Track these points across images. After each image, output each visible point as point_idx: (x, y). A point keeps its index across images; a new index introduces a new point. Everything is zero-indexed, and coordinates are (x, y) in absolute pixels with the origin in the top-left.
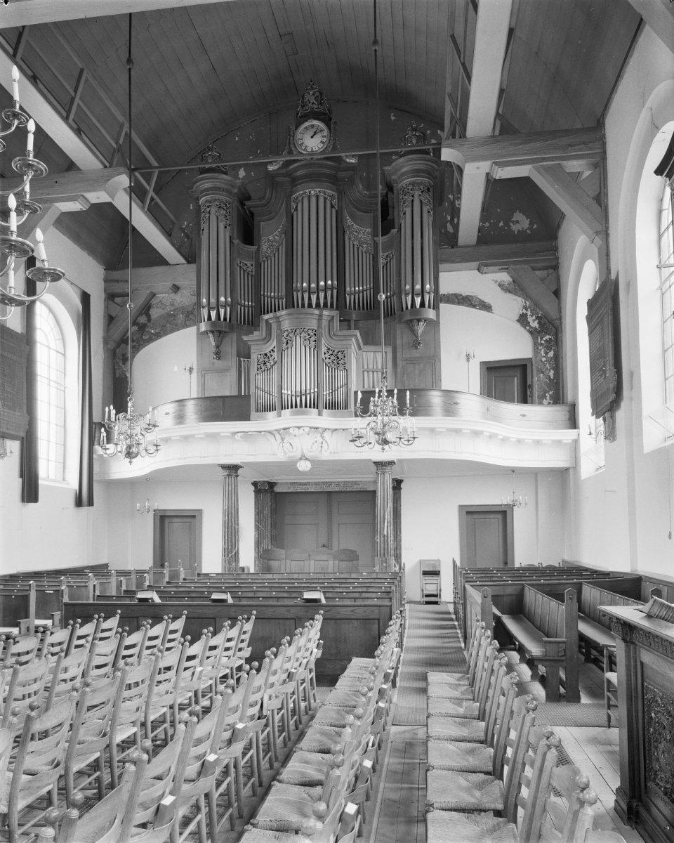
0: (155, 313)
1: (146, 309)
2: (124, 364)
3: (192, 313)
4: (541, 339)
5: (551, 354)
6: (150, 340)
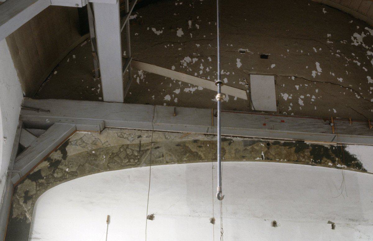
0: (71, 150)
1: (63, 147)
2: (25, 202)
6: (64, 178)
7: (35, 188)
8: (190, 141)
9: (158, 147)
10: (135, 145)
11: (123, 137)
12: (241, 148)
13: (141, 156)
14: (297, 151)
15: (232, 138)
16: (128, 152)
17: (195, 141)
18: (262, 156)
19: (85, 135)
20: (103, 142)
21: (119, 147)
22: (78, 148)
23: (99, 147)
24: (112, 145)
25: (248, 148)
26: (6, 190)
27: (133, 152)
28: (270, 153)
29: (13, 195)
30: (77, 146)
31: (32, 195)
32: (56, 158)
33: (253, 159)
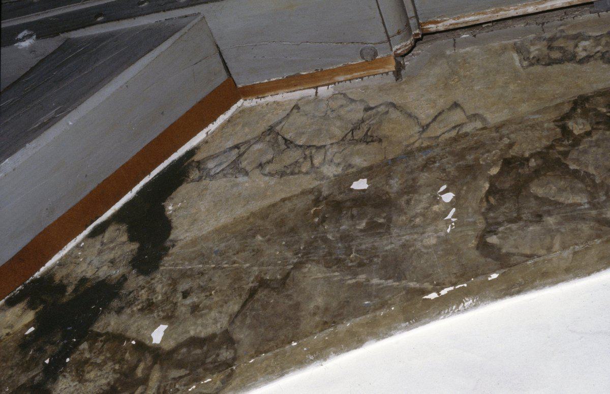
19: (297, 107)
20: (425, 113)
21: (554, 115)
24: (493, 118)
30: (241, 179)
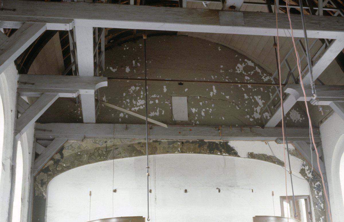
1: (60, 151)
2: (42, 186)
3: (93, 155)
4: (314, 184)
5: (321, 194)
6: (62, 171)
7: (46, 177)
8: (136, 143)
9: (117, 148)
10: (104, 147)
11: (96, 143)
12: (167, 146)
13: (107, 154)
14: (200, 146)
15: (161, 140)
16: (100, 152)
17: (139, 143)
18: (179, 150)
21: (94, 149)
22: (70, 151)
23: (82, 150)
24: (90, 148)
25: (170, 146)
26: (31, 182)
27: (102, 152)
28: (184, 149)
29: (34, 182)
31: (45, 182)
32: (57, 158)
33: (174, 152)
